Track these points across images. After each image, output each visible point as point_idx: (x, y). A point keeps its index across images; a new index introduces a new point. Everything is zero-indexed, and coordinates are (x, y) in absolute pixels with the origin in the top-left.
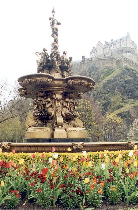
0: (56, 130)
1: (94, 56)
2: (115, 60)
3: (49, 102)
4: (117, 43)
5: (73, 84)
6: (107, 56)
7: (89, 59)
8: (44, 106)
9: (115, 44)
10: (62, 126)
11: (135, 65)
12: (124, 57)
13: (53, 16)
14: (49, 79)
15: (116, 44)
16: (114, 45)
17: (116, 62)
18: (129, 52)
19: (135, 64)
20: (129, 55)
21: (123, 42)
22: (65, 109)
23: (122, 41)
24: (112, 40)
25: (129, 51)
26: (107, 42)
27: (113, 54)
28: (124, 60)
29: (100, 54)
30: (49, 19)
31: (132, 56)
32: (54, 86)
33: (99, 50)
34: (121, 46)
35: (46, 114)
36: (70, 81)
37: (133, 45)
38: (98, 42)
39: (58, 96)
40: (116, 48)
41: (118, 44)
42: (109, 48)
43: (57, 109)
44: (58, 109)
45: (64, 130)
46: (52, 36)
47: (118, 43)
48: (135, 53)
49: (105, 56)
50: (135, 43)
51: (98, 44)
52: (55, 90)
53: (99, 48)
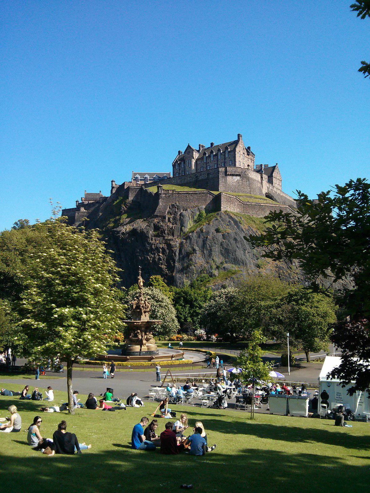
0: (142, 347)
1: (179, 170)
2: (211, 196)
6: (201, 178)
7: (168, 190)
18: (236, 175)
19: (242, 202)
20: (236, 180)
24: (212, 144)
26: (203, 146)
28: (224, 198)
31: (241, 181)
34: (225, 159)
37: (248, 156)
45: (146, 347)
50: (251, 150)
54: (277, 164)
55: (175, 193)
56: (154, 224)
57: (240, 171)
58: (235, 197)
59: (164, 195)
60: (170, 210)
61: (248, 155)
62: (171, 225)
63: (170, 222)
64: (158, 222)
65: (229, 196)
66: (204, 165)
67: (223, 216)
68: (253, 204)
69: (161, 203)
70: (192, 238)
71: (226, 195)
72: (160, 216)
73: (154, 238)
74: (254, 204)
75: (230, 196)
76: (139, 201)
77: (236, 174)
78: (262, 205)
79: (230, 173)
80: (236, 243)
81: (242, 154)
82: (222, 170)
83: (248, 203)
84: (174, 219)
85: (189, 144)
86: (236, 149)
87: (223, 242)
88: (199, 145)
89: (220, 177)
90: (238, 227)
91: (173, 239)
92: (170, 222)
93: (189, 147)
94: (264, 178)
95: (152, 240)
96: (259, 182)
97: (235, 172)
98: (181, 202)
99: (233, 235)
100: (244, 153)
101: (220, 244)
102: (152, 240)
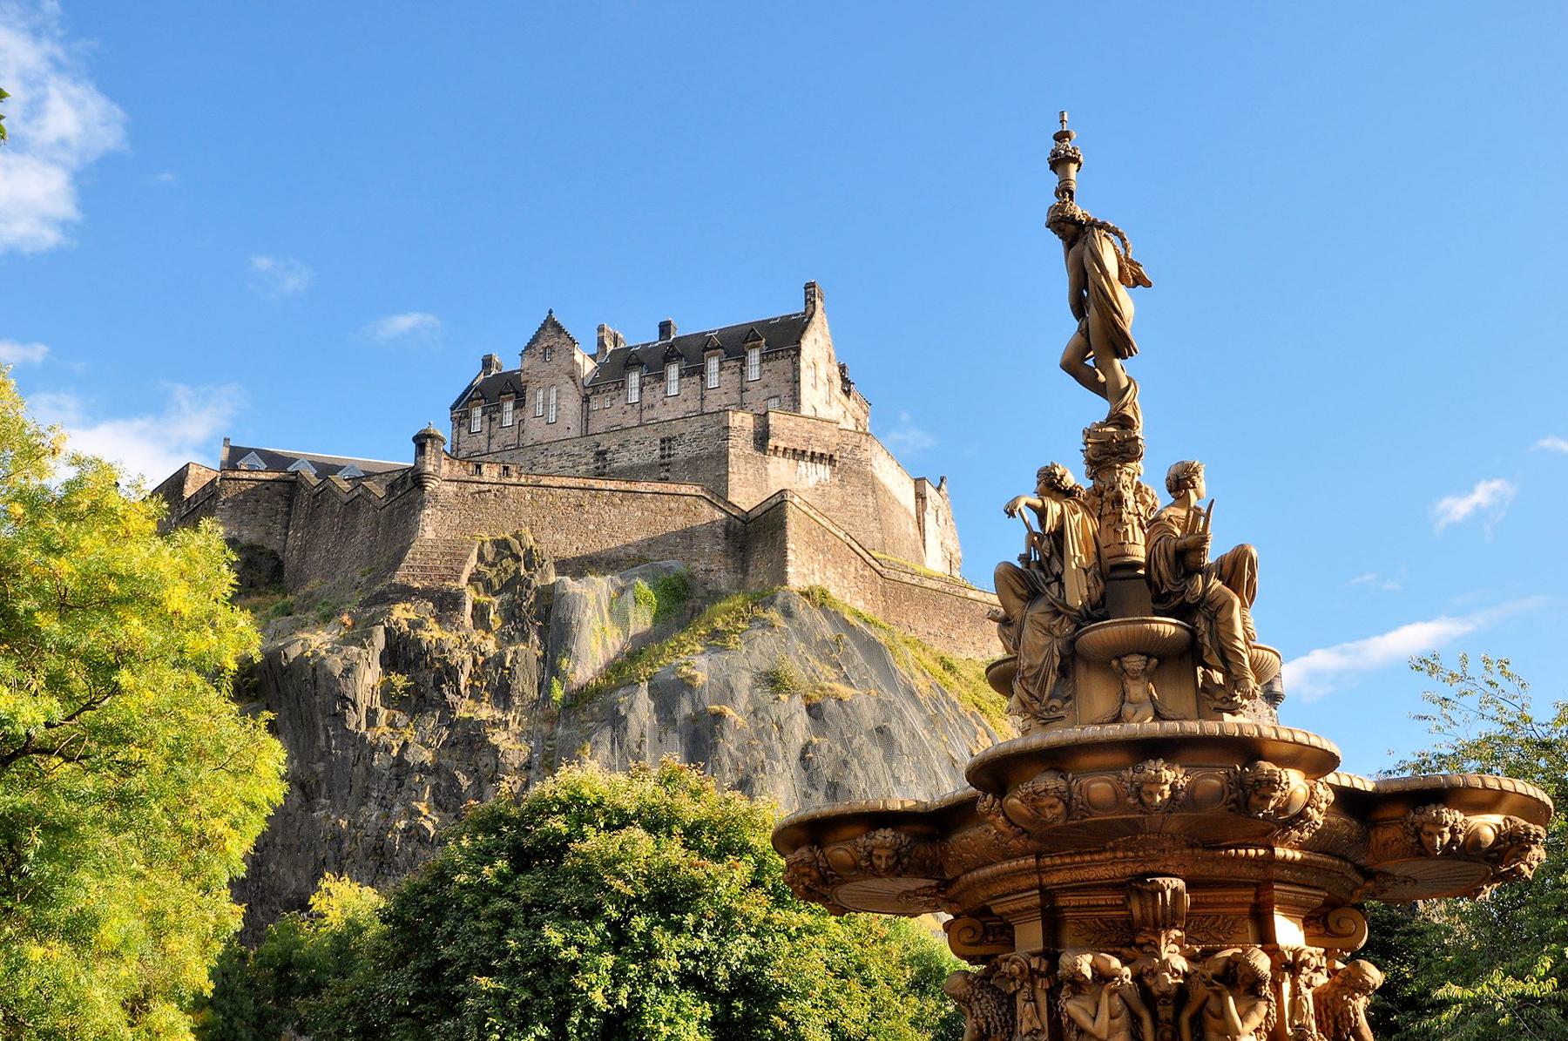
1: (490, 438)
4: (713, 364)
5: (1453, 841)
6: (623, 460)
9: (699, 371)
11: (880, 580)
12: (796, 500)
13: (1065, 191)
15: (702, 373)
16: (681, 376)
17: (719, 530)
19: (879, 568)
20: (811, 481)
21: (764, 365)
23: (754, 356)
24: (665, 328)
25: (818, 450)
27: (681, 452)
28: (797, 522)
29: (551, 434)
30: (1044, 219)
31: (836, 490)
33: (540, 397)
34: (743, 391)
37: (843, 397)
38: (543, 327)
40: (693, 405)
41: (720, 370)
42: (634, 397)
46: (1074, 366)
47: (720, 363)
48: (866, 474)
49: (601, 455)
51: (535, 339)
53: (548, 381)
54: (942, 480)
55: (514, 480)
56: (388, 632)
57: (835, 441)
58: (842, 535)
59: (451, 488)
60: (482, 568)
61: (847, 393)
62: (490, 646)
63: (488, 629)
64: (416, 625)
65: (821, 521)
66: (629, 415)
67: (801, 607)
68: (928, 583)
69: (431, 527)
70: (631, 717)
71: (805, 508)
72: (425, 594)
73: (383, 713)
74: (935, 587)
75: (825, 524)
76: (275, 547)
77: (813, 453)
78: (971, 595)
79: (782, 445)
80: (889, 757)
81: (824, 377)
82: (742, 422)
83: (907, 578)
84: (511, 613)
85: (551, 312)
86: (803, 347)
87: (817, 748)
88: (601, 329)
89: (731, 457)
90: (888, 673)
91: (510, 717)
92: (488, 629)
93: (551, 326)
94: (928, 500)
95: (371, 723)
96: (909, 514)
97: (808, 440)
98: (549, 531)
99: (870, 716)
100: (830, 381)
101: (794, 755)
102: (371, 723)
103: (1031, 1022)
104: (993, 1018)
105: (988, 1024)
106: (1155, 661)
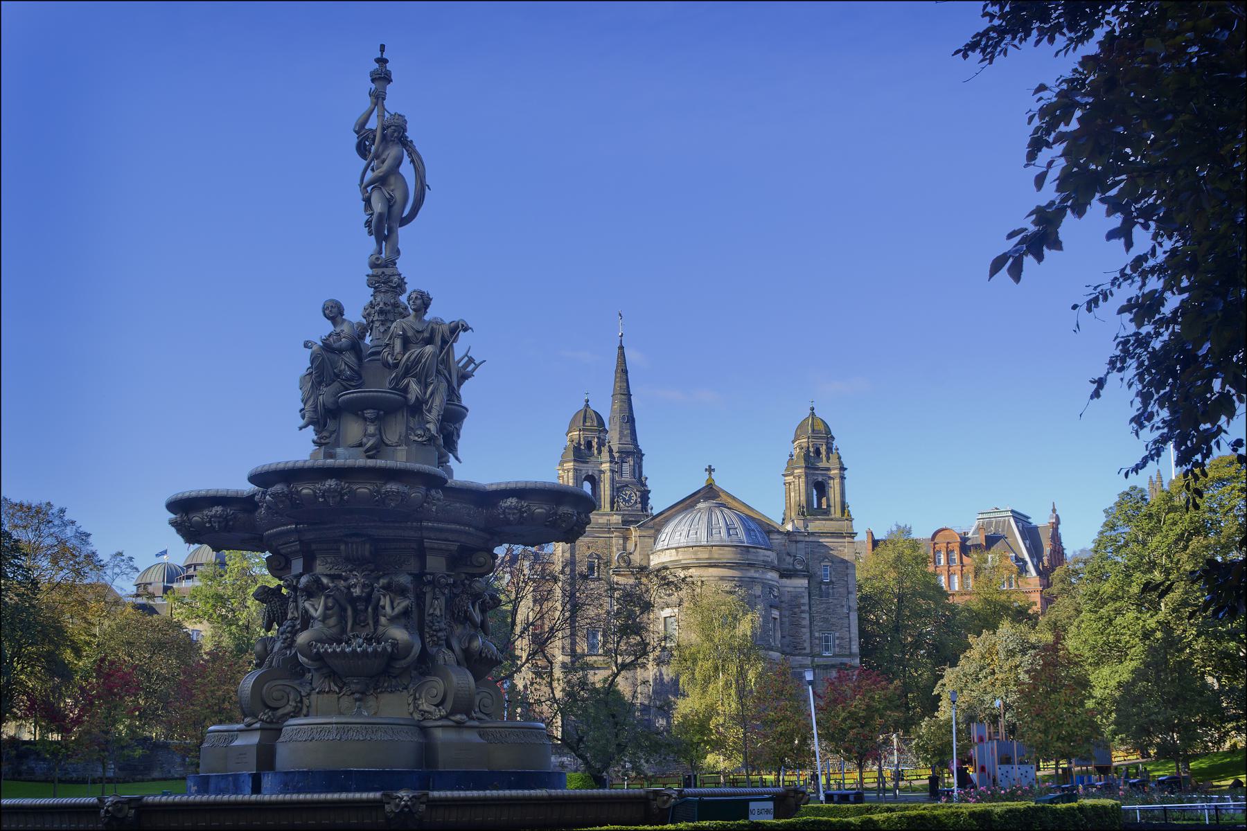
3: (402, 592)
8: (355, 610)
10: (467, 716)
14: (433, 492)
22: (458, 630)
32: (429, 520)
35: (389, 649)
36: (512, 501)
39: (436, 564)
43: (435, 631)
44: (440, 630)
52: (432, 535)
103: (292, 613)
104: (277, 611)
105: (275, 614)
106: (382, 413)
